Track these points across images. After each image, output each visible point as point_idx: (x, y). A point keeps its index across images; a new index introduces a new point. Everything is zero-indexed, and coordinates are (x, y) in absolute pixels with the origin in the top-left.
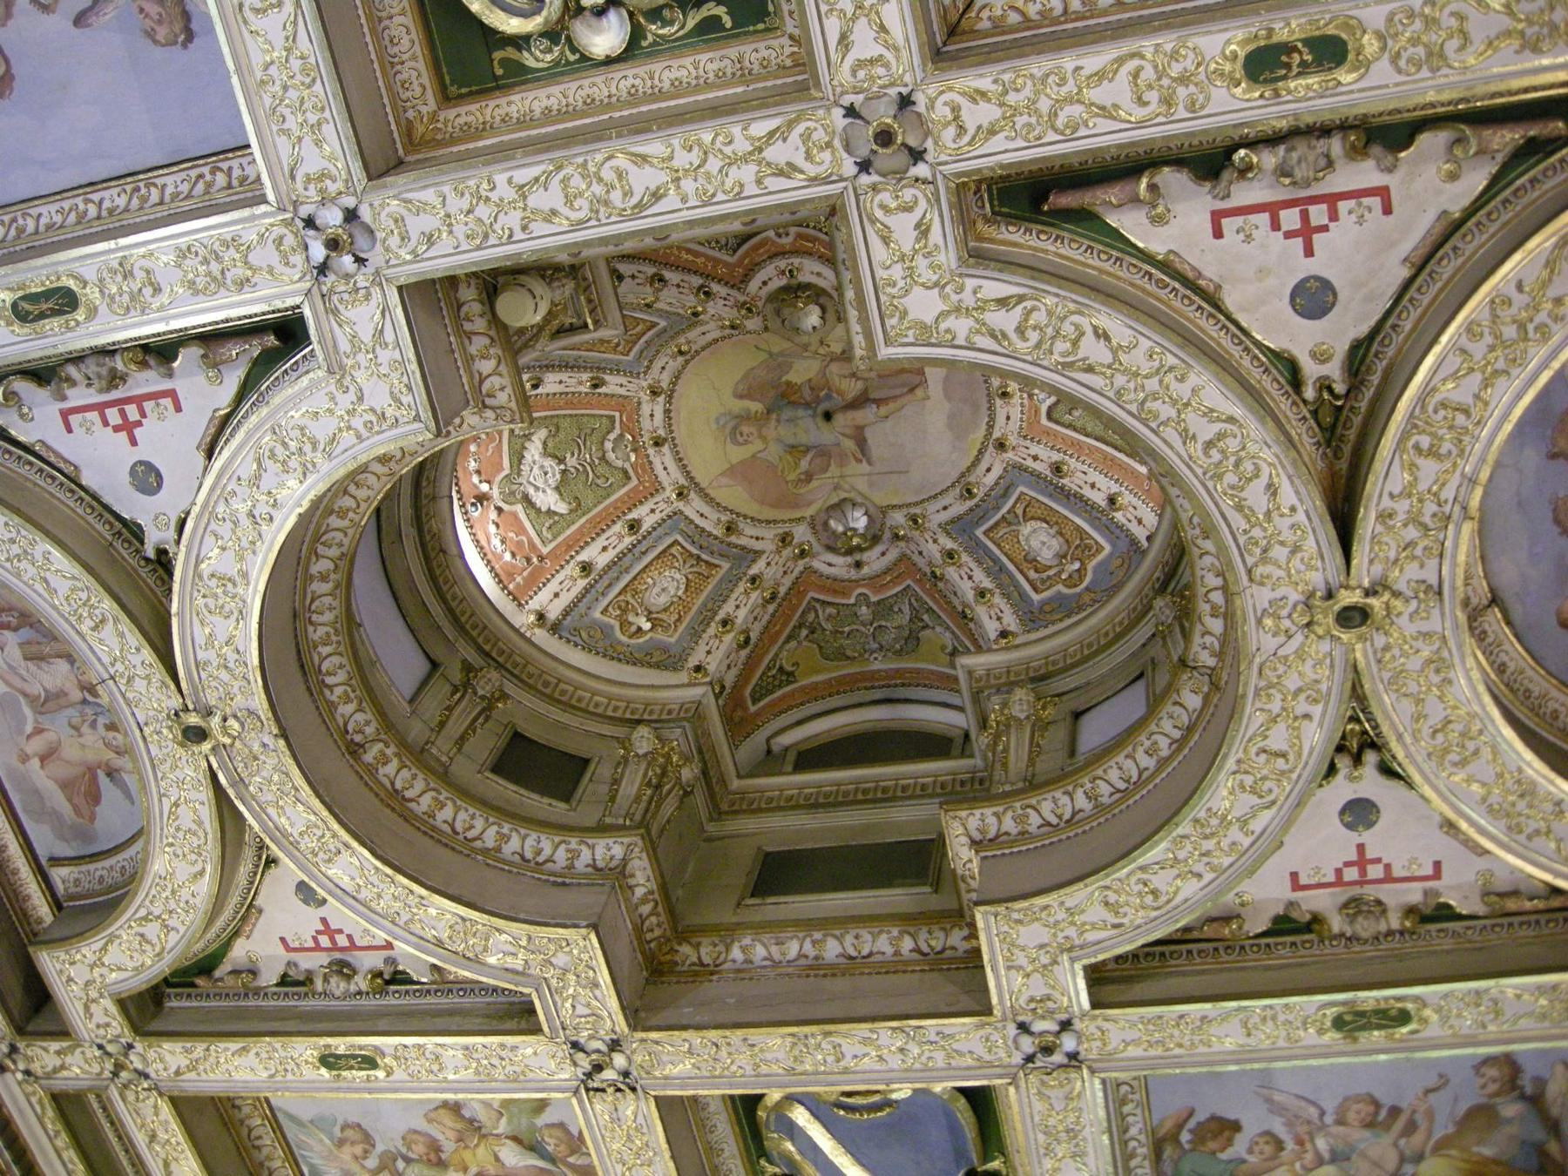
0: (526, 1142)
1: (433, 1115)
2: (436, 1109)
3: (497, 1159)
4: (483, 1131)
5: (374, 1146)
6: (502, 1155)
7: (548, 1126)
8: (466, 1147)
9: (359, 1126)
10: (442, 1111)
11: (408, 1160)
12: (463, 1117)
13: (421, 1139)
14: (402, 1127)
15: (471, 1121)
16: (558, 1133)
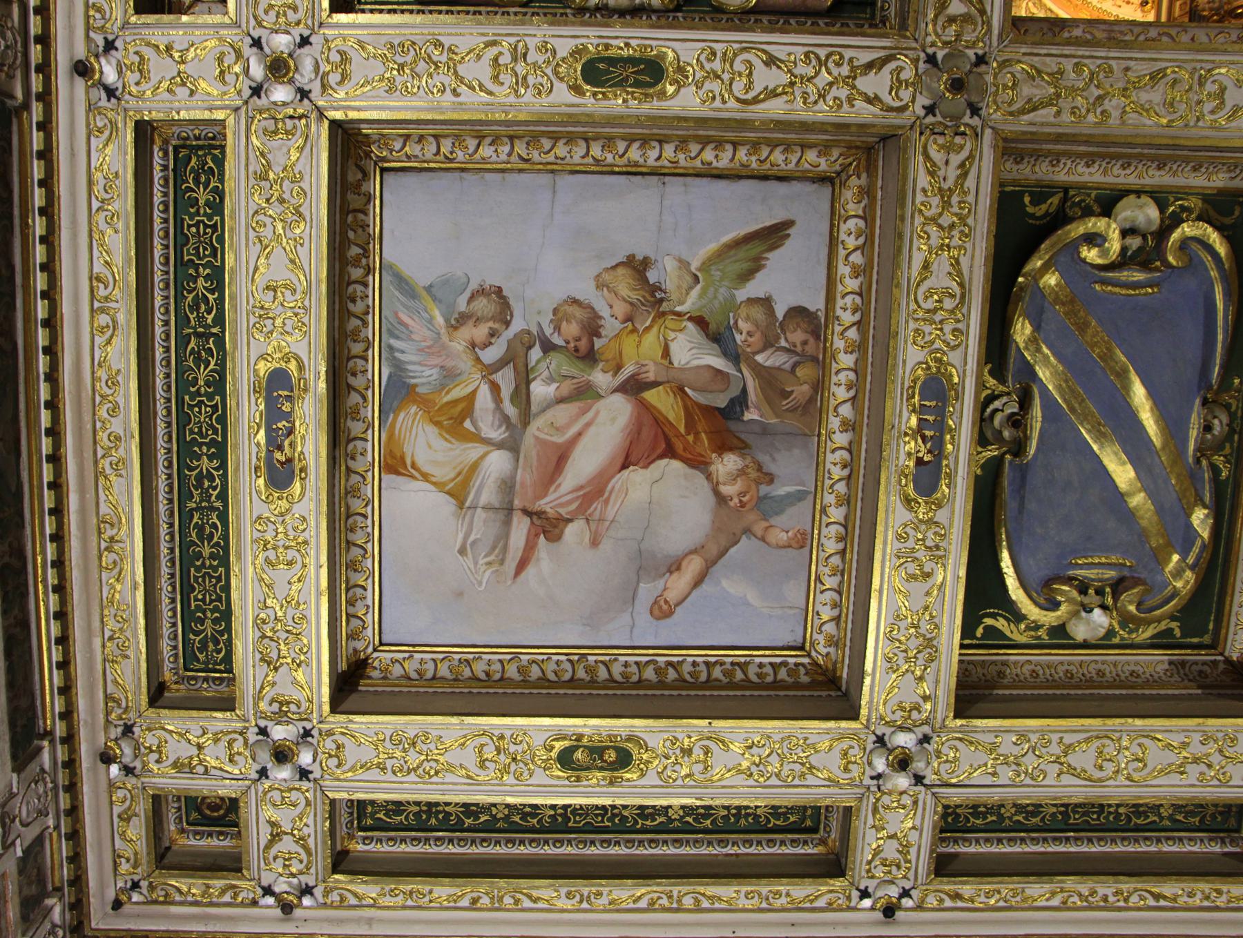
0: (713, 327)
1: (606, 277)
2: (614, 267)
3: (666, 353)
4: (665, 307)
5: (507, 324)
6: (673, 347)
7: (751, 301)
8: (634, 330)
9: (499, 291)
10: (621, 271)
11: (548, 347)
12: (645, 280)
13: (578, 312)
14: (558, 293)
15: (656, 288)
16: (758, 313)
